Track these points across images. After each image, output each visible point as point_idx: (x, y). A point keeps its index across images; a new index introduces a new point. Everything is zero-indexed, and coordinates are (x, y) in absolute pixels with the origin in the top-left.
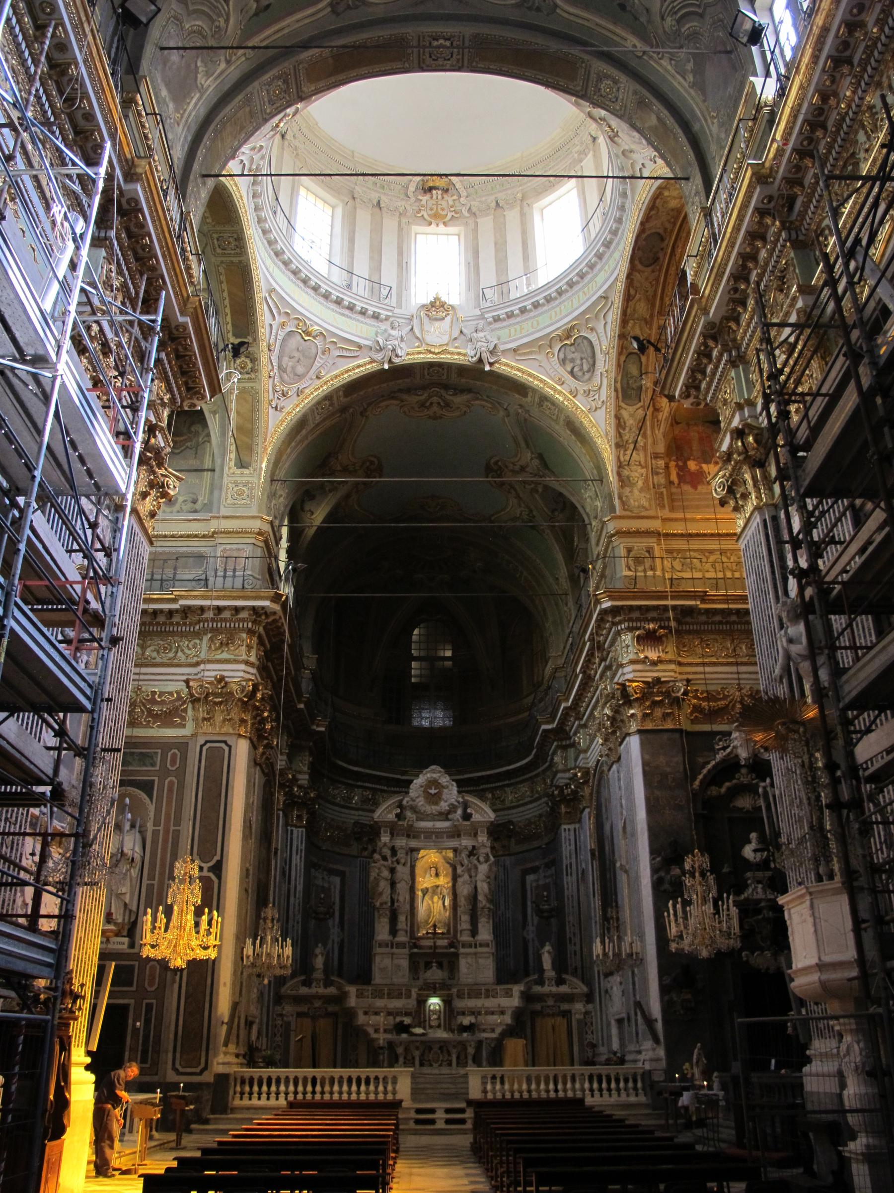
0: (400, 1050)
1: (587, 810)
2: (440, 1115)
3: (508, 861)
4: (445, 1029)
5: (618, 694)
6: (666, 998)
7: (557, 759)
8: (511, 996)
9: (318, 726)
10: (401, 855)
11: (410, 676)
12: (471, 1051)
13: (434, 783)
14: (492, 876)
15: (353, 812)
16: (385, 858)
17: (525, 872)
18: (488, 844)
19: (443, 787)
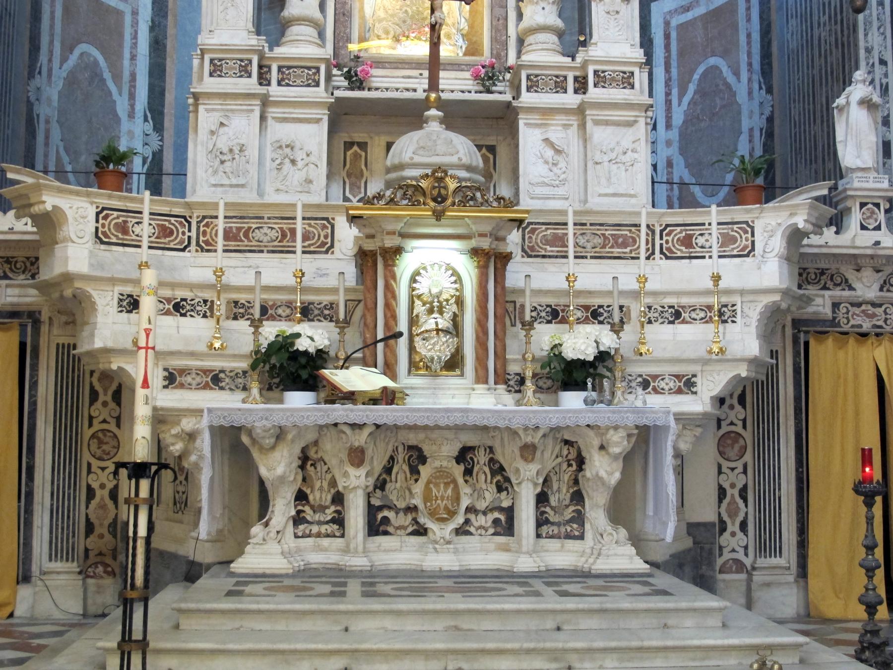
0: (276, 467)
4: (481, 378)
8: (749, 252)
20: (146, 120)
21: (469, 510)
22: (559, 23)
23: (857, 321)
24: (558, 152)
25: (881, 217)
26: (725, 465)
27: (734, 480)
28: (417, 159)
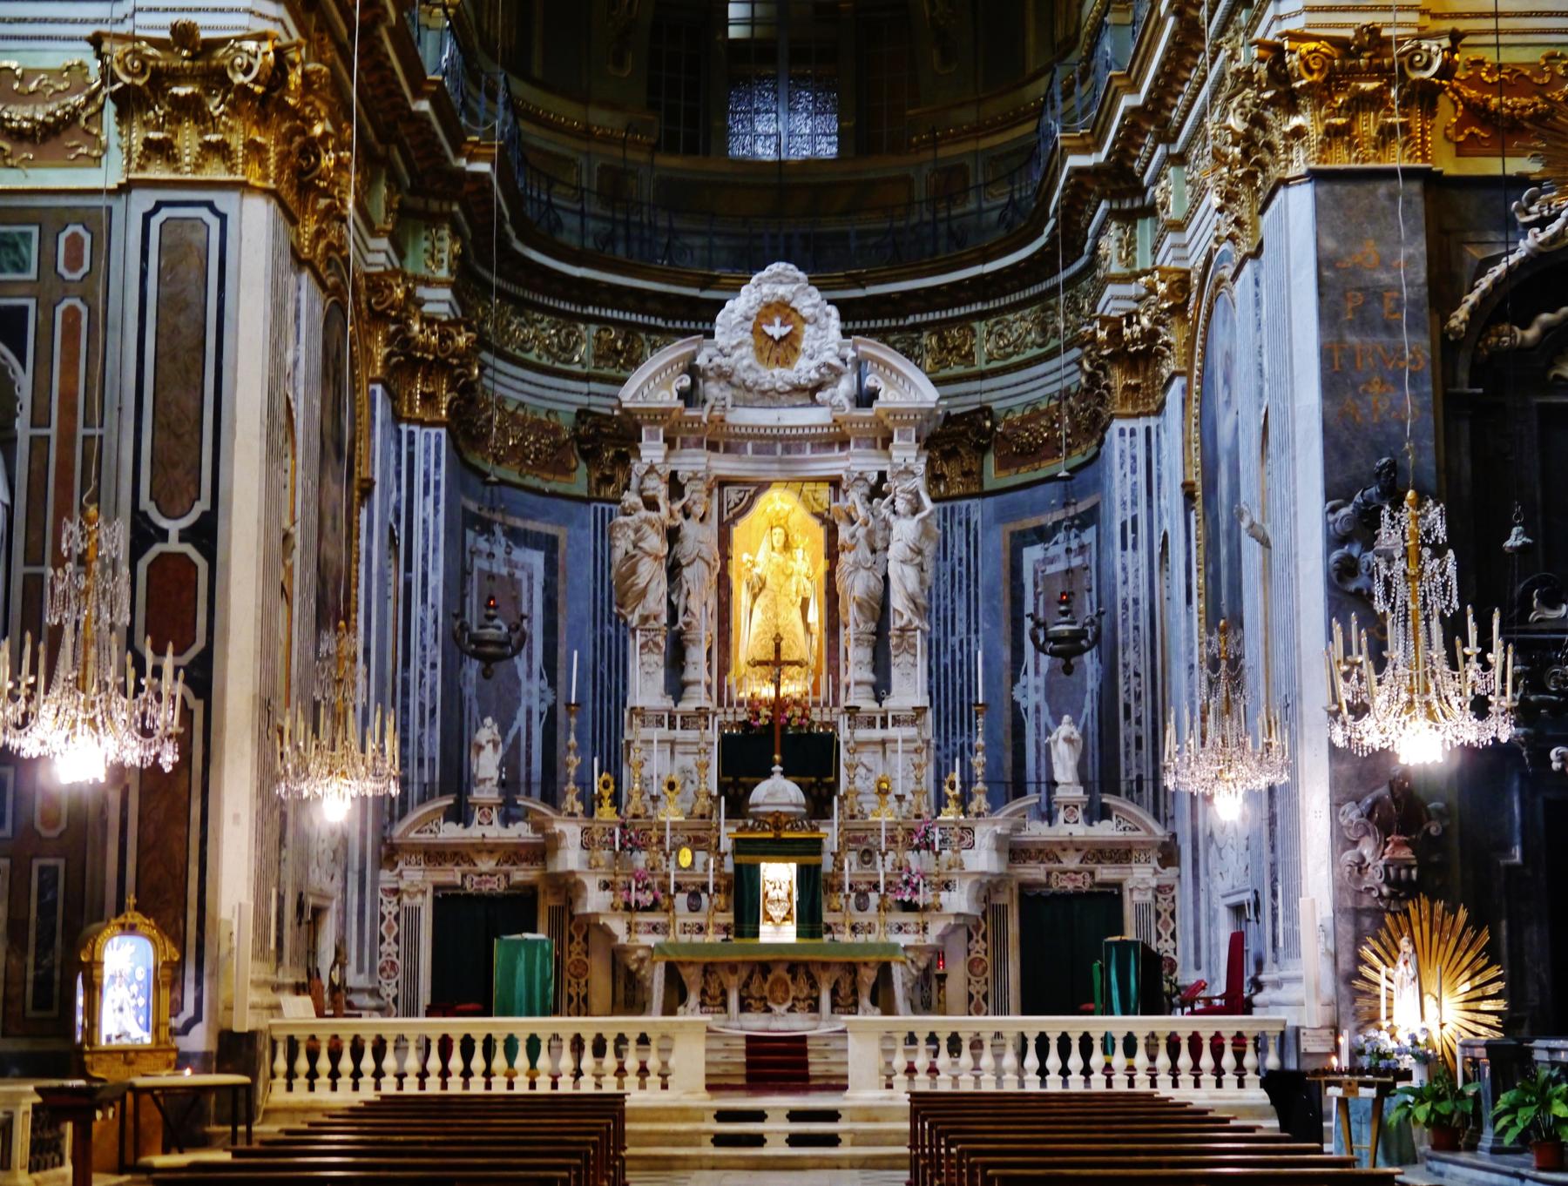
1: (1178, 384)
2: (777, 1128)
3: (978, 510)
5: (1262, 70)
6: (1350, 856)
7: (1109, 244)
9: (472, 158)
10: (694, 494)
11: (725, 23)
12: (868, 976)
13: (782, 309)
14: (929, 549)
15: (572, 385)
16: (651, 504)
17: (1020, 541)
18: (920, 467)
19: (804, 320)
20: (541, 677)
21: (795, 998)
22: (870, 677)
23: (1064, 883)
24: (869, 770)
25: (1079, 814)
26: (973, 979)
27: (978, 989)
28: (768, 800)
